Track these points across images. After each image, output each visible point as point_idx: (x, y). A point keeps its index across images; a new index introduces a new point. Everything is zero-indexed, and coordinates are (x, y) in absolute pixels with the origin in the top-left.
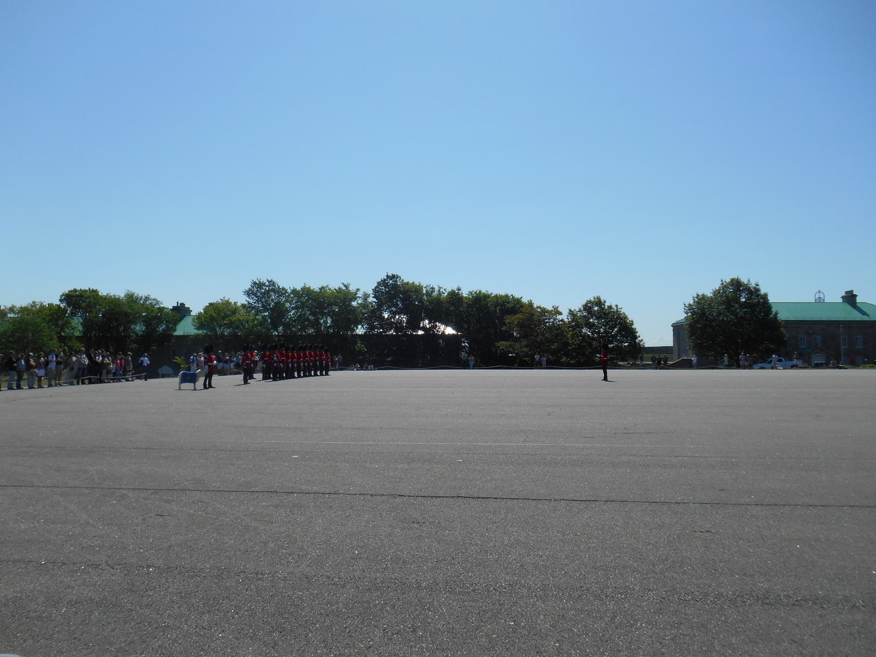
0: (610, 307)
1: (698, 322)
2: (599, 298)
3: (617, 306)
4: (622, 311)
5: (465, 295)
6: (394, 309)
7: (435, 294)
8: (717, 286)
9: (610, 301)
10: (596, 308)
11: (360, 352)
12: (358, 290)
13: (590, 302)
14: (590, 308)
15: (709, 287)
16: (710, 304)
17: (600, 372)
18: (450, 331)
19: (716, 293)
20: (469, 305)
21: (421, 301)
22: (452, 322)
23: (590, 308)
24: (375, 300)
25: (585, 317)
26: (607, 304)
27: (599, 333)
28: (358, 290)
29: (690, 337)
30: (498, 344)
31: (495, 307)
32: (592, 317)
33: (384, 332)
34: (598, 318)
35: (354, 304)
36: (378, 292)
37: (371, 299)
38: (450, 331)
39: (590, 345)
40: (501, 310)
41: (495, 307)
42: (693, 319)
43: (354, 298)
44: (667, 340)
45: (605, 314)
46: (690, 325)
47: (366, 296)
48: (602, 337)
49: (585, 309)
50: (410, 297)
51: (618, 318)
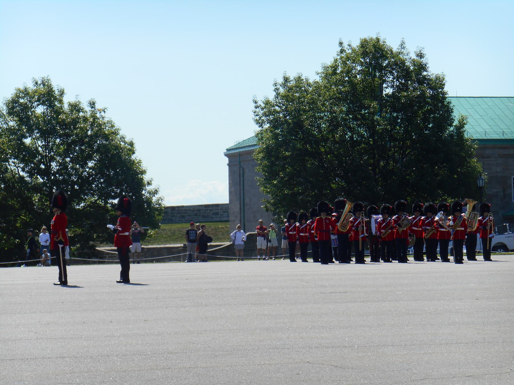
0: (75, 107)
1: (286, 144)
2: (46, 83)
3: (92, 104)
4: (108, 116)
8: (329, 56)
9: (75, 91)
10: (40, 110)
13: (26, 92)
14: (25, 108)
15: (311, 61)
16: (313, 102)
17: (53, 272)
19: (330, 73)
23: (25, 108)
25: (11, 131)
26: (68, 99)
27: (46, 173)
29: (268, 180)
32: (30, 131)
34: (45, 134)
39: (27, 204)
42: (276, 136)
44: (213, 188)
45: (63, 124)
46: (270, 153)
48: (56, 182)
49: (11, 113)
51: (96, 136)
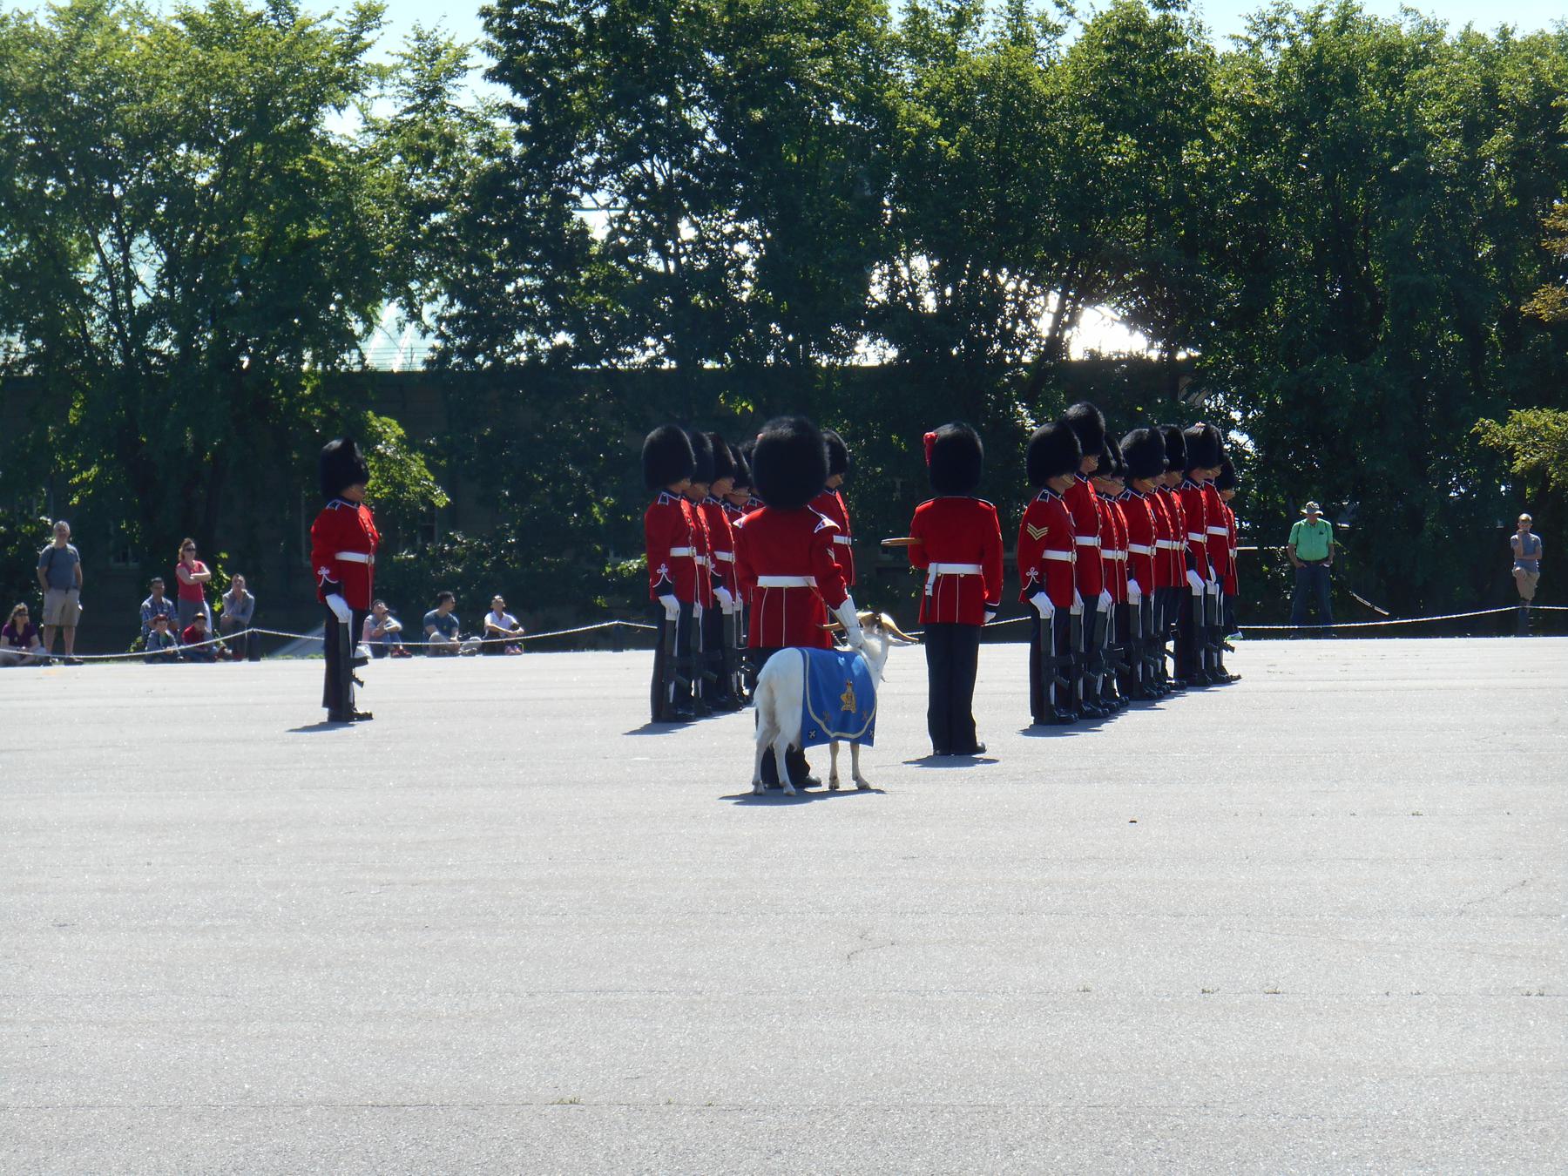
5: (1222, 47)
6: (660, 170)
7: (984, 39)
11: (402, 518)
12: (368, 17)
18: (1104, 333)
20: (1258, 127)
21: (866, 104)
22: (1121, 263)
24: (504, 93)
28: (368, 17)
30: (1492, 432)
31: (1474, 131)
33: (585, 351)
35: (341, 125)
36: (525, 31)
37: (477, 91)
38: (1104, 333)
40: (1519, 158)
41: (1474, 131)
43: (339, 77)
47: (434, 67)
50: (785, 61)
